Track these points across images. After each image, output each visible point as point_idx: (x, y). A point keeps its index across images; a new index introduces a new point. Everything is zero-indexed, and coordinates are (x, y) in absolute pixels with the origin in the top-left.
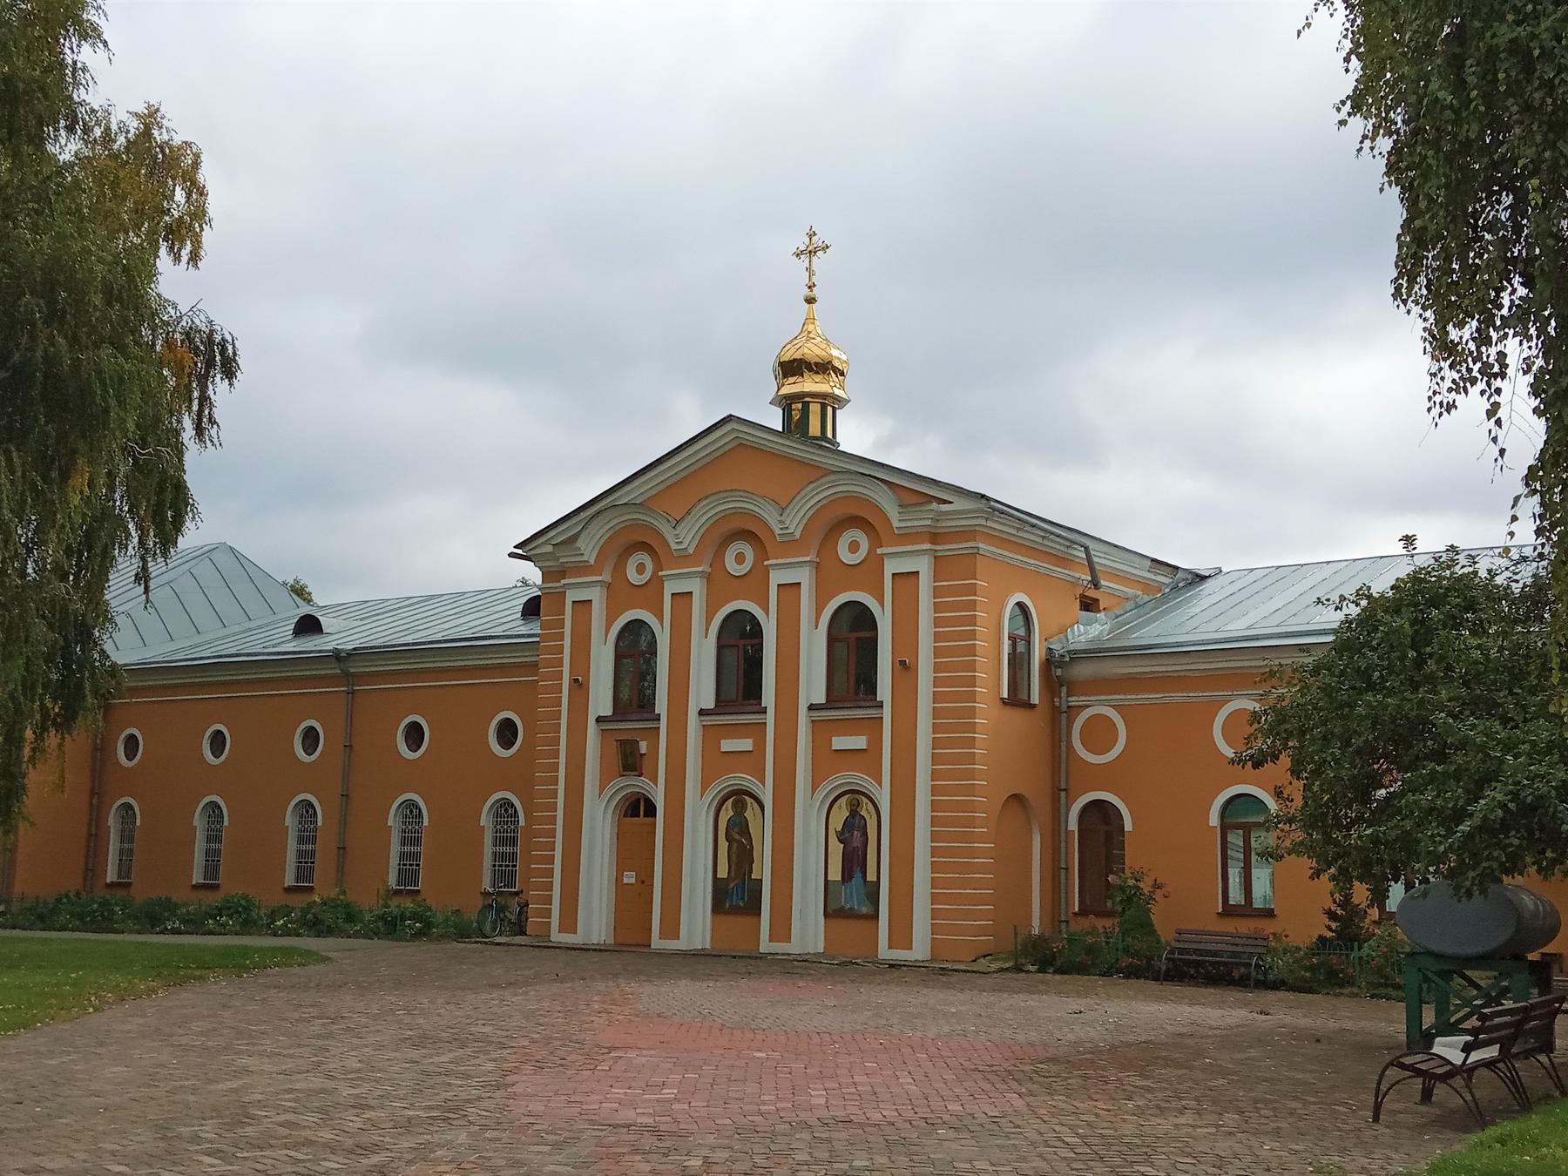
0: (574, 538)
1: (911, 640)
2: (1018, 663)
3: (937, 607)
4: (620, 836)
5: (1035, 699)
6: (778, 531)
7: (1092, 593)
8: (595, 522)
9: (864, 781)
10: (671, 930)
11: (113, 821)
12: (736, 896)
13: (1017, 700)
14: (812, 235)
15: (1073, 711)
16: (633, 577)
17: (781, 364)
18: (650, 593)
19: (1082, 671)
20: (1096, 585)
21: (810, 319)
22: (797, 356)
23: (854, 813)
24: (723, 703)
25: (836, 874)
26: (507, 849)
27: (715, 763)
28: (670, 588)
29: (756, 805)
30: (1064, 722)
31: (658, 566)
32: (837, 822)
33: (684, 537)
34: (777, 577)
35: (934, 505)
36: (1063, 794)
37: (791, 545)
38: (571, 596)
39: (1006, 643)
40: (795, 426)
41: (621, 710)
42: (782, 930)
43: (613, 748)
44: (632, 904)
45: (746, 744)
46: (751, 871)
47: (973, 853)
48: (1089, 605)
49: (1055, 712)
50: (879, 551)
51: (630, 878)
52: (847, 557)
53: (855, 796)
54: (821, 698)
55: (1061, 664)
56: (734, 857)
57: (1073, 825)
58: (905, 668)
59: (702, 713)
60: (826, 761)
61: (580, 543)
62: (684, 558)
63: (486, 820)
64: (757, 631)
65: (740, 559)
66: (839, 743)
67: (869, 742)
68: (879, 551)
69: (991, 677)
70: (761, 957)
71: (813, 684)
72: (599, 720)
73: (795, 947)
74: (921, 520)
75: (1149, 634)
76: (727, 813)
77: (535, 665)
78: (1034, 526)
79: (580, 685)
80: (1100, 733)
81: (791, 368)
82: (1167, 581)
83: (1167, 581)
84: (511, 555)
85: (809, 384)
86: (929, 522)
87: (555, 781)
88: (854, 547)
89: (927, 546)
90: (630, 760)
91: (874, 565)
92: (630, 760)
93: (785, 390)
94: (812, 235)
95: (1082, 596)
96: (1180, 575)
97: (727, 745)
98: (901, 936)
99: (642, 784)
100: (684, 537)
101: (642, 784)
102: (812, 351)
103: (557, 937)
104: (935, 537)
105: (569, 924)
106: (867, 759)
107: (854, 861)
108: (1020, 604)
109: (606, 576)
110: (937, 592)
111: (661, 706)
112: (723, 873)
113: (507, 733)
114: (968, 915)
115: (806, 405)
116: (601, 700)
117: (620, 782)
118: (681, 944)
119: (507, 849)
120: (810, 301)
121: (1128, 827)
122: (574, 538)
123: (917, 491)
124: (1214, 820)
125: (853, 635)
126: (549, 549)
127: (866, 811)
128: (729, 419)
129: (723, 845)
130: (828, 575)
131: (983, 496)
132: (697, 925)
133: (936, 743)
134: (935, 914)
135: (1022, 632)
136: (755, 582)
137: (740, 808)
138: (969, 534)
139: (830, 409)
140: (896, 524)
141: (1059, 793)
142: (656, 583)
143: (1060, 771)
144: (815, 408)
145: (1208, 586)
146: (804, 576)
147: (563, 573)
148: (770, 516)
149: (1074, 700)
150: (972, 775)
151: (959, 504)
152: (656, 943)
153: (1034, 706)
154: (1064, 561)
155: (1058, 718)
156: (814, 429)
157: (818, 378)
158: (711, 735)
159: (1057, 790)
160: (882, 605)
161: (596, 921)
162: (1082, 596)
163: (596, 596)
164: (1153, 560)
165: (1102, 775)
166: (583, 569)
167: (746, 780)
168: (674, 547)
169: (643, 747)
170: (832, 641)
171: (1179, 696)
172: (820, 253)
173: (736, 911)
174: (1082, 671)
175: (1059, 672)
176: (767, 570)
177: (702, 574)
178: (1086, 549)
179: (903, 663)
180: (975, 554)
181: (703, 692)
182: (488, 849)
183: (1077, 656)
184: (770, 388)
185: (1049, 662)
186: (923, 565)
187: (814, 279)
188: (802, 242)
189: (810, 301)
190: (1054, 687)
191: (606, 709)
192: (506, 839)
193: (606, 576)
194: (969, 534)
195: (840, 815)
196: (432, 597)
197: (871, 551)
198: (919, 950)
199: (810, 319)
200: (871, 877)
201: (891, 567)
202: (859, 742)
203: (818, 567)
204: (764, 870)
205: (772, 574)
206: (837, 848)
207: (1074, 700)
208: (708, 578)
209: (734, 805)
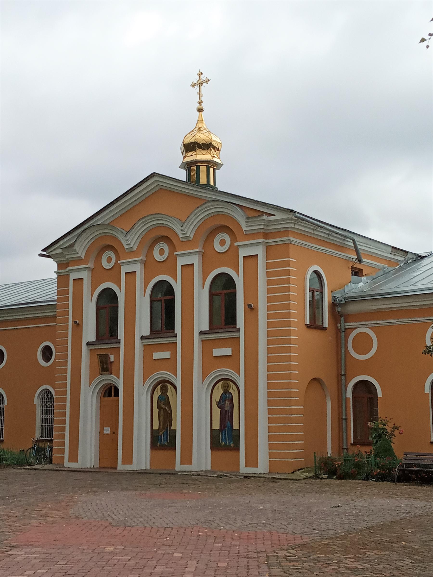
0: (72, 245)
1: (256, 293)
2: (316, 305)
3: (268, 274)
4: (102, 407)
5: (326, 325)
6: (181, 236)
7: (358, 266)
8: (84, 235)
9: (230, 373)
10: (128, 459)
12: (163, 439)
13: (315, 325)
14: (200, 74)
15: (348, 331)
16: (105, 264)
17: (184, 145)
18: (114, 273)
19: (352, 308)
21: (200, 121)
22: (193, 140)
23: (226, 391)
24: (154, 332)
25: (217, 426)
26: (49, 416)
27: (150, 365)
28: (124, 270)
30: (343, 337)
31: (118, 258)
32: (217, 397)
33: (131, 241)
34: (181, 262)
35: (265, 217)
36: (343, 378)
38: (73, 276)
39: (308, 295)
40: (193, 179)
41: (100, 337)
42: (187, 458)
43: (96, 360)
44: (107, 445)
45: (166, 355)
46: (171, 425)
47: (290, 412)
48: (357, 272)
49: (338, 331)
50: (236, 244)
51: (107, 431)
52: (219, 248)
53: (226, 382)
54: (206, 328)
55: (340, 305)
56: (162, 418)
57: (349, 394)
58: (251, 309)
59: (143, 338)
60: (210, 362)
61: (76, 247)
63: (37, 401)
64: (170, 291)
65: (162, 252)
66: (217, 352)
67: (233, 351)
68: (236, 244)
69: (300, 312)
70: (175, 474)
71: (202, 320)
72: (88, 344)
73: (194, 467)
75: (390, 287)
76: (158, 393)
77: (55, 317)
78: (322, 227)
79: (78, 325)
80: (363, 344)
81: (189, 147)
82: (401, 259)
83: (401, 259)
84: (41, 255)
85: (200, 155)
86: (262, 227)
87: (65, 378)
88: (222, 243)
89: (262, 240)
90: (105, 365)
91: (233, 251)
92: (105, 365)
93: (188, 159)
94: (200, 74)
95: (353, 268)
96: (409, 256)
97: (157, 355)
98: (252, 461)
99: (112, 378)
100: (131, 241)
101: (112, 378)
102: (201, 137)
103: (68, 464)
104: (266, 235)
105: (74, 457)
106: (231, 360)
107: (227, 417)
108: (316, 272)
109: (91, 265)
110: (268, 266)
111: (121, 335)
112: (156, 427)
113: (47, 353)
114: (289, 447)
115: (198, 168)
116: (89, 333)
117: (100, 378)
118: (134, 467)
119: (49, 416)
120: (200, 110)
121: (380, 395)
122: (72, 245)
123: (256, 209)
125: (223, 291)
126: (60, 251)
127: (232, 390)
128: (153, 175)
129: (156, 411)
130: (208, 258)
131: (292, 211)
132: (142, 456)
133: (269, 351)
134: (271, 447)
135: (317, 286)
136: (169, 265)
137: (164, 390)
138: (286, 232)
139: (212, 170)
140: (244, 228)
141: (341, 377)
142: (117, 267)
143: (342, 365)
144: (203, 169)
145: (425, 262)
146: (195, 260)
147: (67, 264)
148: (177, 228)
149: (349, 325)
150: (289, 368)
151: (279, 216)
152: (120, 467)
153: (326, 329)
154: (342, 248)
155: (340, 335)
156: (203, 180)
157: (204, 152)
158: (148, 350)
159: (340, 375)
160: (238, 274)
161: (89, 455)
162: (353, 268)
163: (85, 275)
164: (393, 248)
165: (365, 366)
166: (79, 261)
167: (167, 375)
168: (126, 247)
169: (112, 358)
170: (212, 295)
171: (406, 320)
172: (205, 84)
173: (163, 448)
174: (352, 308)
175: (339, 309)
176: (176, 257)
177: (141, 261)
178: (354, 241)
179: (250, 306)
180: (288, 244)
182: (38, 416)
183: (349, 301)
184: (179, 158)
185: (334, 304)
186: (260, 251)
187: (202, 99)
188: (195, 79)
189: (200, 110)
190: (336, 318)
191: (92, 338)
192: (48, 411)
193: (91, 265)
194: (286, 232)
195: (218, 392)
196: (18, 284)
197: (232, 245)
198: (263, 467)
199: (200, 121)
200: (235, 427)
201: (243, 253)
202: (228, 351)
203: (203, 254)
204: (177, 425)
206: (217, 411)
207: (349, 325)
208: (145, 263)
209: (161, 389)
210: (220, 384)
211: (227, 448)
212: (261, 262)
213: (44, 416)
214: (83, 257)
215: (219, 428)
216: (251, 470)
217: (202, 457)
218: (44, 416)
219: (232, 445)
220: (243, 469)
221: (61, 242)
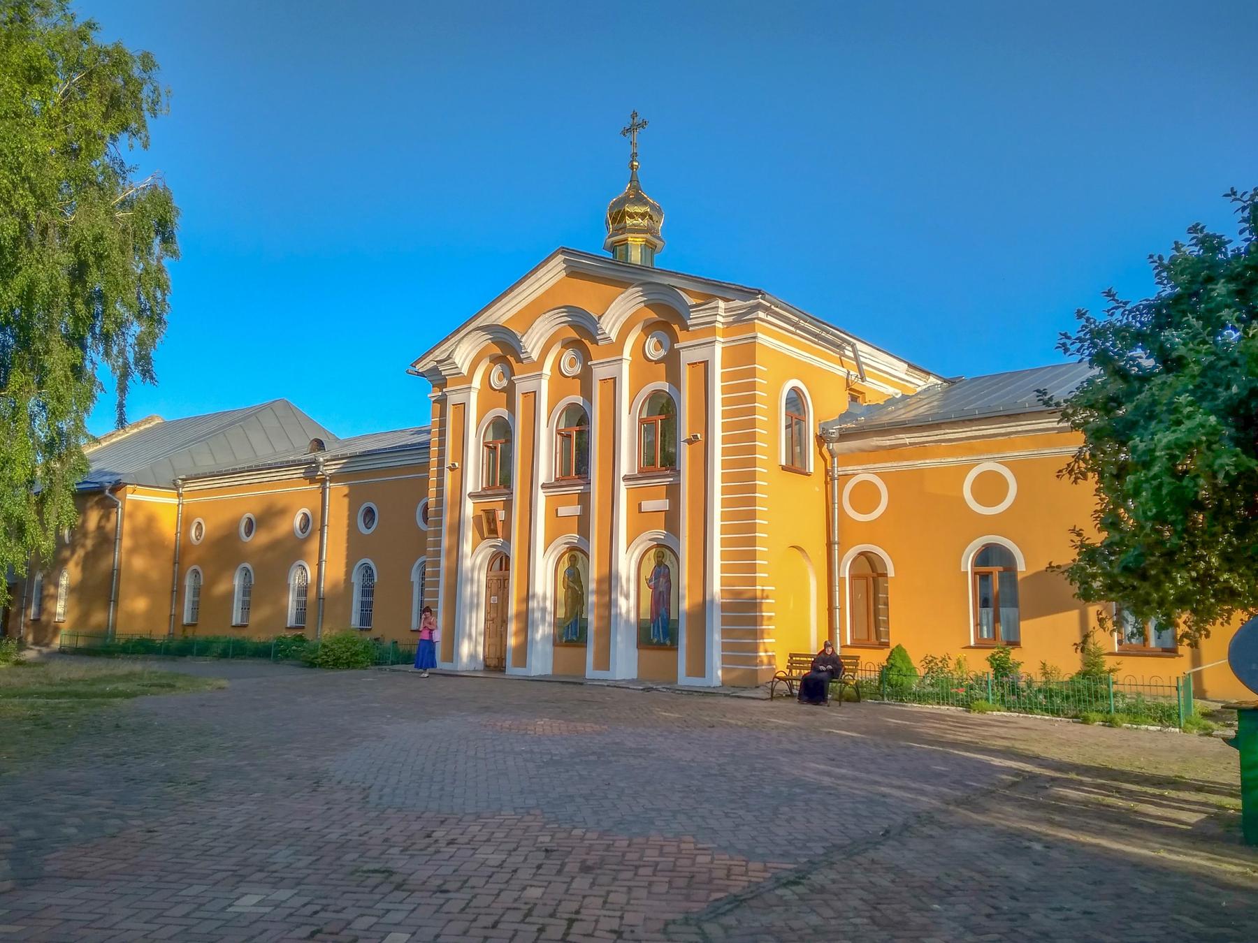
0: (449, 357)
11: (189, 582)
13: (795, 466)
14: (634, 115)
20: (863, 379)
42: (604, 661)
49: (829, 477)
50: (676, 346)
68: (676, 346)
76: (565, 565)
94: (634, 115)
121: (891, 573)
122: (449, 357)
124: (968, 565)
178: (853, 346)
181: (545, 469)
206: (647, 593)
211: (660, 646)
213: (364, 599)
216: (696, 682)
217: (625, 662)
218: (364, 599)
219: (668, 642)
220: (684, 680)
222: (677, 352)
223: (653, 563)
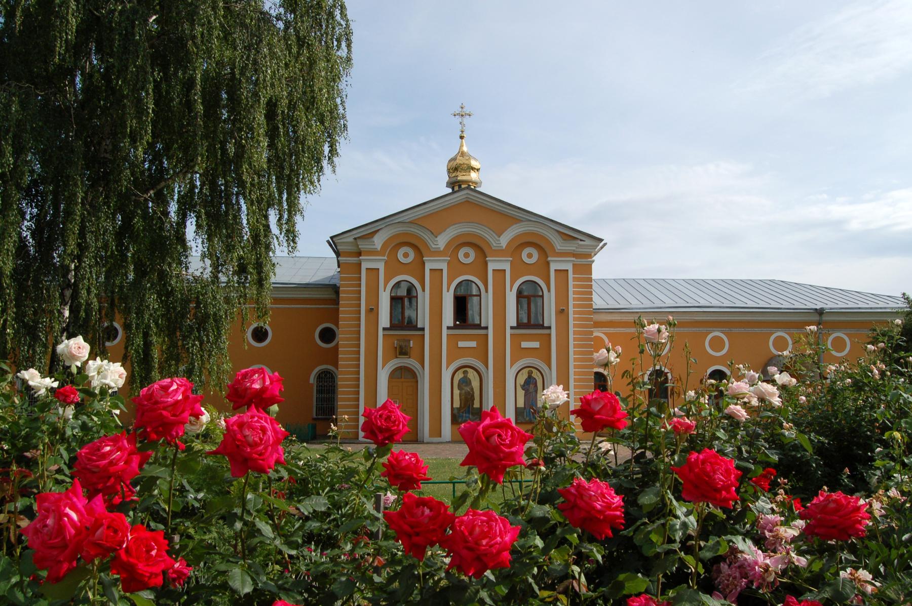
29: (475, 373)
37: (500, 253)
38: (364, 266)
60: (519, 353)
62: (437, 253)
72: (384, 329)
74: (571, 247)
79: (373, 311)
84: (328, 242)
100: (442, 242)
104: (575, 255)
116: (384, 320)
125: (529, 297)
129: (457, 392)
151: (588, 242)
205: (489, 264)
210: (527, 370)
212: (571, 275)
214: (379, 248)
215: (523, 406)
221: (354, 232)
222: (548, 264)
223: (526, 376)
